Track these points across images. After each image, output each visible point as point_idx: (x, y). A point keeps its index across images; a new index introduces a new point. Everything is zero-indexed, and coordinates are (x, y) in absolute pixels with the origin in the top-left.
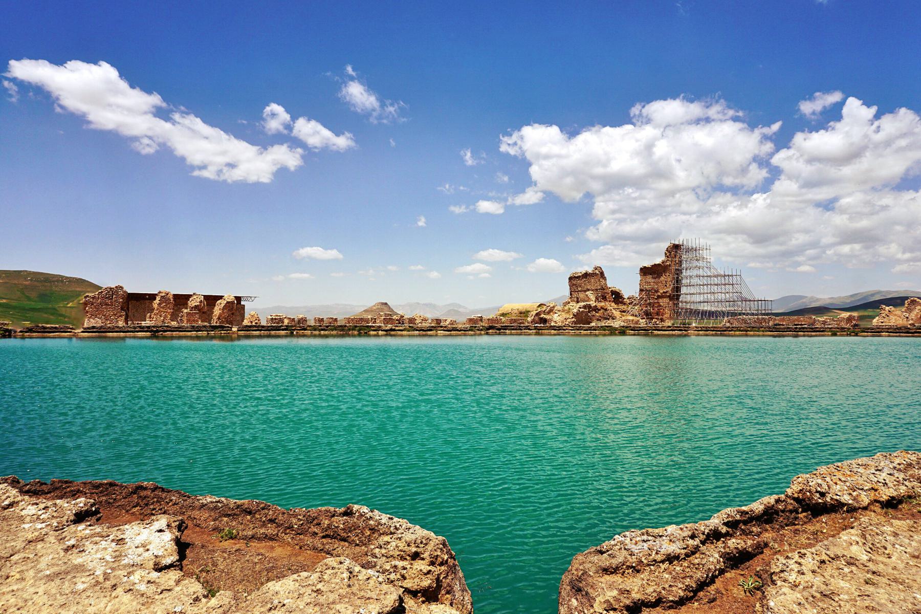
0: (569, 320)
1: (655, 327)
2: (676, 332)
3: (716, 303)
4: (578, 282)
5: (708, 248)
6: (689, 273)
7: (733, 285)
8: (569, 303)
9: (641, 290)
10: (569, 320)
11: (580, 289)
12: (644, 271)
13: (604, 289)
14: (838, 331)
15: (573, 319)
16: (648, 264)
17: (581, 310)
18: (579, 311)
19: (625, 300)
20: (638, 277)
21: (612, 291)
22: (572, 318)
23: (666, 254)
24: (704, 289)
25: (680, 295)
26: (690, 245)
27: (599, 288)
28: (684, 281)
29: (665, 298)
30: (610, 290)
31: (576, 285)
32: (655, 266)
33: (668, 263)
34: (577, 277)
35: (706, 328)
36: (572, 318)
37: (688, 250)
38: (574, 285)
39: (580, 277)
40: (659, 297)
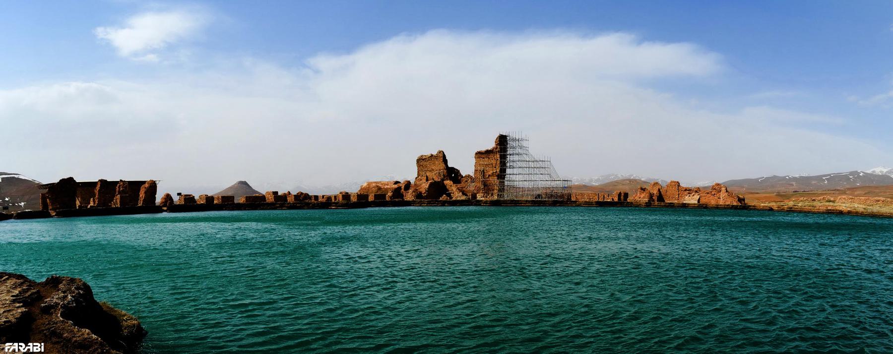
5: (527, 139)
9: (476, 171)
12: (479, 154)
16: (483, 149)
20: (474, 161)
24: (529, 171)
25: (506, 175)
26: (514, 136)
28: (508, 165)
34: (423, 160)
37: (514, 140)
39: (426, 159)
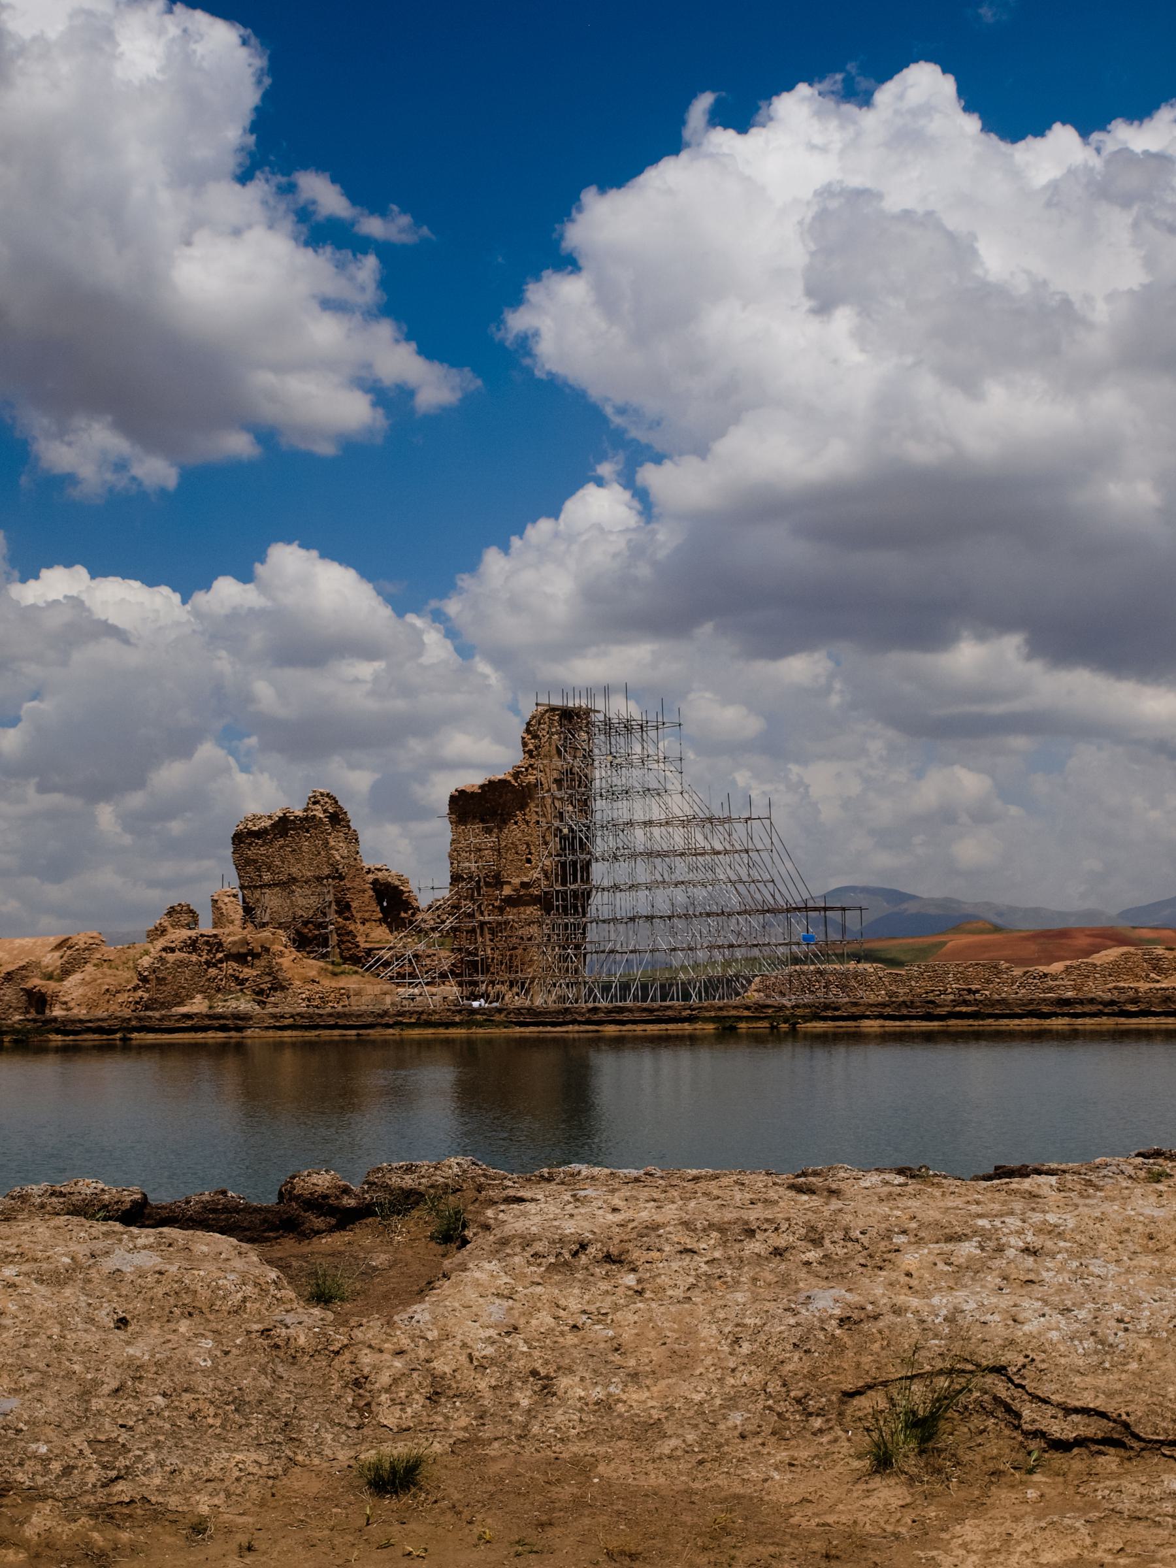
0: (121, 998)
1: (140, 1019)
2: (210, 1034)
3: (680, 924)
4: (263, 850)
6: (622, 810)
7: (747, 851)
8: (164, 932)
9: (456, 879)
10: (121, 998)
11: (267, 877)
13: (341, 878)
14: (740, 1019)
15: (140, 993)
17: (171, 957)
18: (161, 959)
19: (419, 917)
21: (375, 882)
22: (135, 989)
23: (525, 744)
27: (326, 871)
29: (527, 904)
30: (371, 877)
31: (255, 861)
32: (492, 787)
33: (531, 779)
35: (311, 1017)
36: (135, 989)
38: (249, 862)
40: (510, 901)
